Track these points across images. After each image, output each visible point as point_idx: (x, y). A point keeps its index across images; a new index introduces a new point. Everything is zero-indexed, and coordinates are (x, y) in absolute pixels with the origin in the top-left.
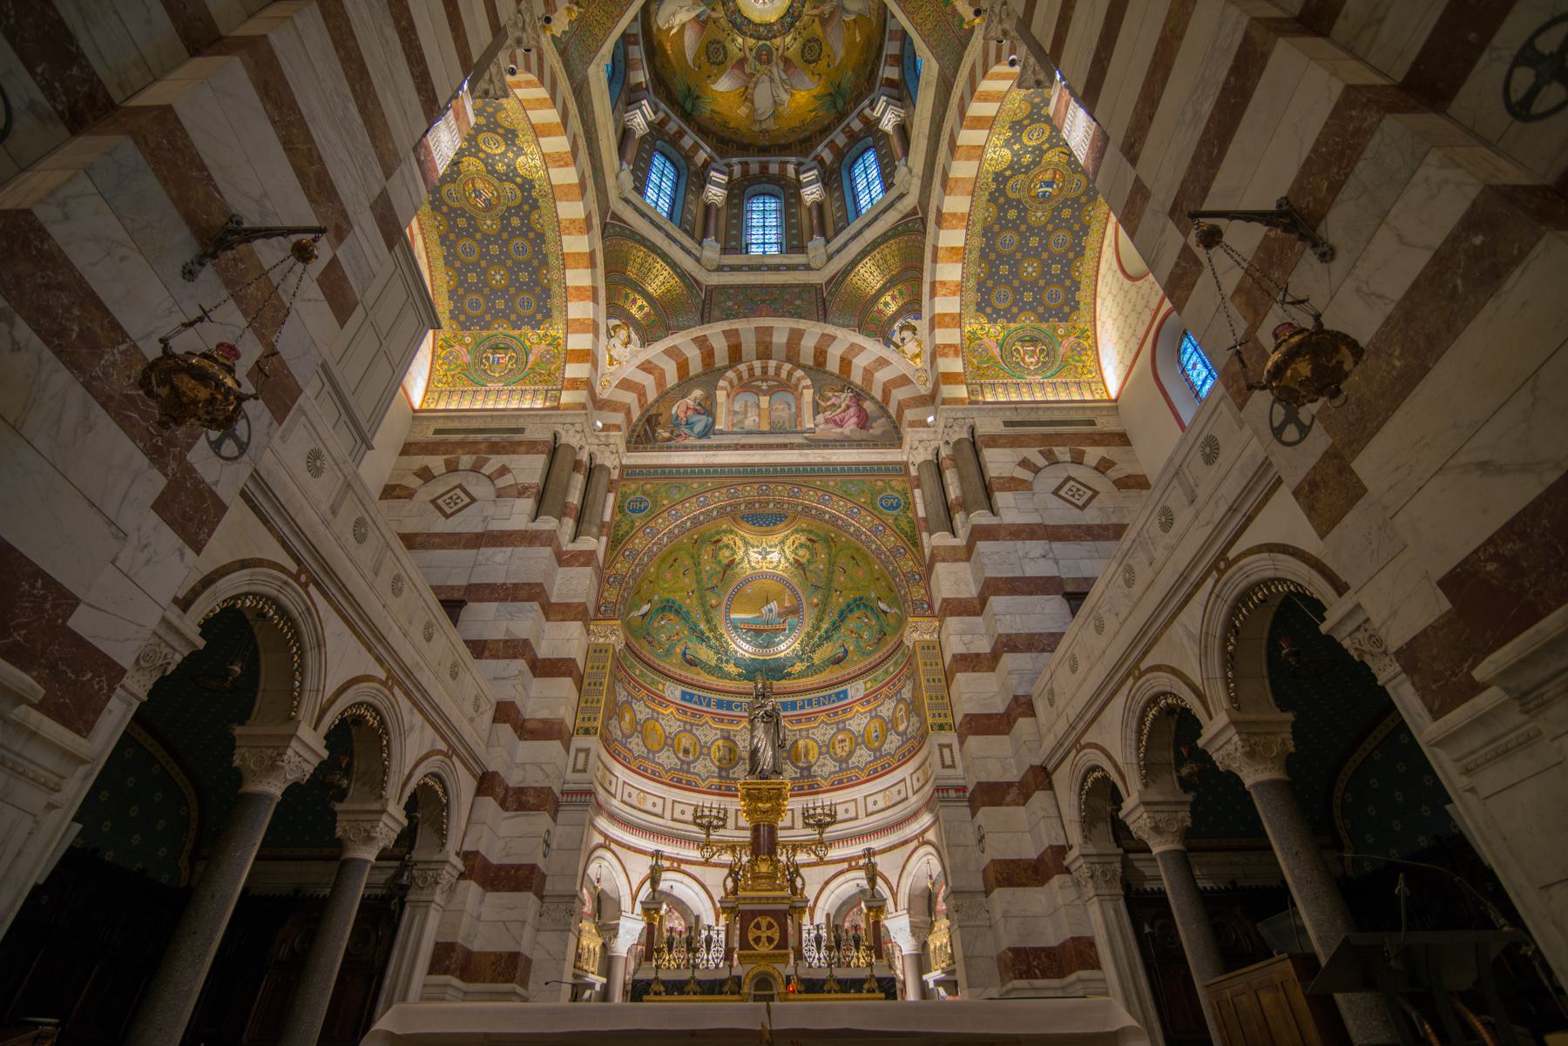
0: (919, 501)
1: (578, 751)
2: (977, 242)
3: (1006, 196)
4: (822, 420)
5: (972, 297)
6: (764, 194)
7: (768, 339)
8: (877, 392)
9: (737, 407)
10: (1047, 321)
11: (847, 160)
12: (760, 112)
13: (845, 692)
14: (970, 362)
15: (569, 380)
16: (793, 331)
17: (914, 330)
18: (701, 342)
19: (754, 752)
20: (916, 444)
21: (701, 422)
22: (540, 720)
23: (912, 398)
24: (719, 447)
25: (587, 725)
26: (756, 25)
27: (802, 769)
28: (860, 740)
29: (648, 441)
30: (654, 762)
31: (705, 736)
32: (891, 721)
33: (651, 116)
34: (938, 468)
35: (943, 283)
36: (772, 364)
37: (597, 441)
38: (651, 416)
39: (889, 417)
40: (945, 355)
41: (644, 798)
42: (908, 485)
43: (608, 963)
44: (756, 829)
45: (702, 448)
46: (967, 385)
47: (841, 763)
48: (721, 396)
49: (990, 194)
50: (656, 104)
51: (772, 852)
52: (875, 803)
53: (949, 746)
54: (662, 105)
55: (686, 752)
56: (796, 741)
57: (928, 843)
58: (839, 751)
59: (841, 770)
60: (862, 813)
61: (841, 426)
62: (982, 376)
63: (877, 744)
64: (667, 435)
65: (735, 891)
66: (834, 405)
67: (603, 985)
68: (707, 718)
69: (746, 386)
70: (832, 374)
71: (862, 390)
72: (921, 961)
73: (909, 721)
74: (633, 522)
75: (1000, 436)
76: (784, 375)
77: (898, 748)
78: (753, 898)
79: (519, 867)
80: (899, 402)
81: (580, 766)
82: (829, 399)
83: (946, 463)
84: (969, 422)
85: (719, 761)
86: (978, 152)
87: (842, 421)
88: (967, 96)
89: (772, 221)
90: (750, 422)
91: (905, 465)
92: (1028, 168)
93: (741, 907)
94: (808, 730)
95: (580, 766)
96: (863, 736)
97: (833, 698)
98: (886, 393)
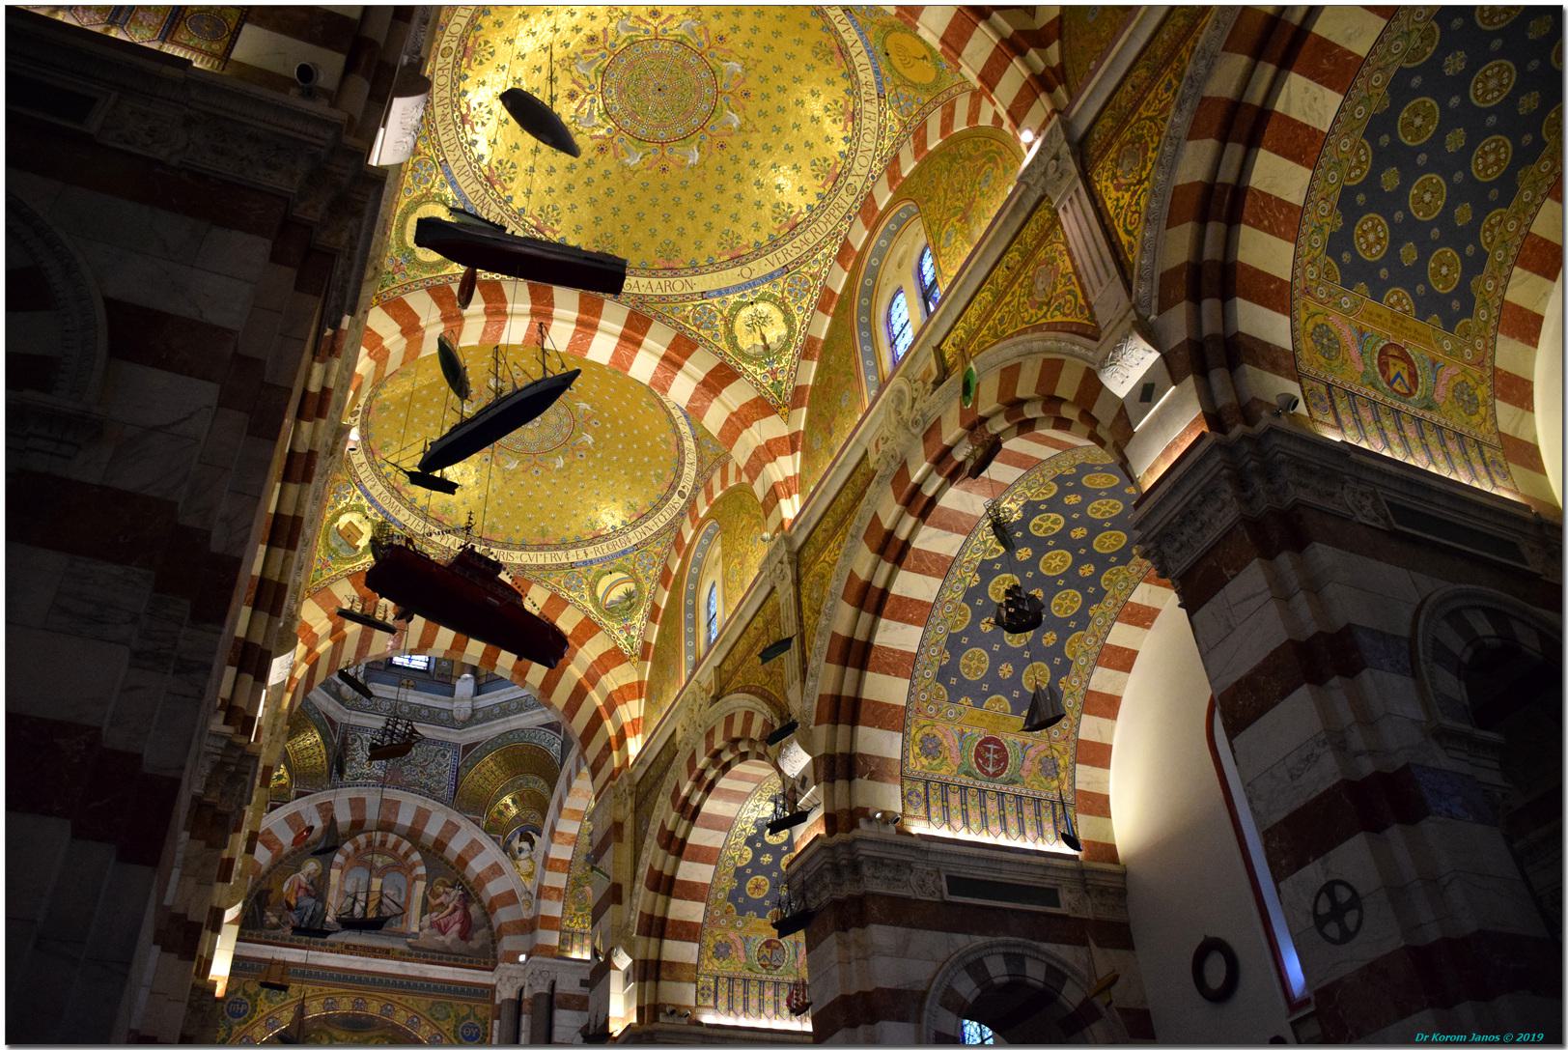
0: (495, 1033)
7: (393, 820)
16: (419, 808)
17: (532, 843)
18: (326, 810)
23: (514, 922)
34: (518, 1004)
35: (562, 834)
36: (392, 838)
38: (262, 892)
39: (491, 928)
40: (549, 898)
42: (489, 1013)
46: (561, 931)
48: (335, 874)
61: (444, 933)
64: (274, 920)
66: (442, 904)
69: (358, 859)
70: (447, 862)
71: (472, 889)
74: (231, 1029)
75: (574, 996)
82: (439, 896)
83: (526, 1007)
84: (552, 976)
87: (446, 926)
91: (492, 988)
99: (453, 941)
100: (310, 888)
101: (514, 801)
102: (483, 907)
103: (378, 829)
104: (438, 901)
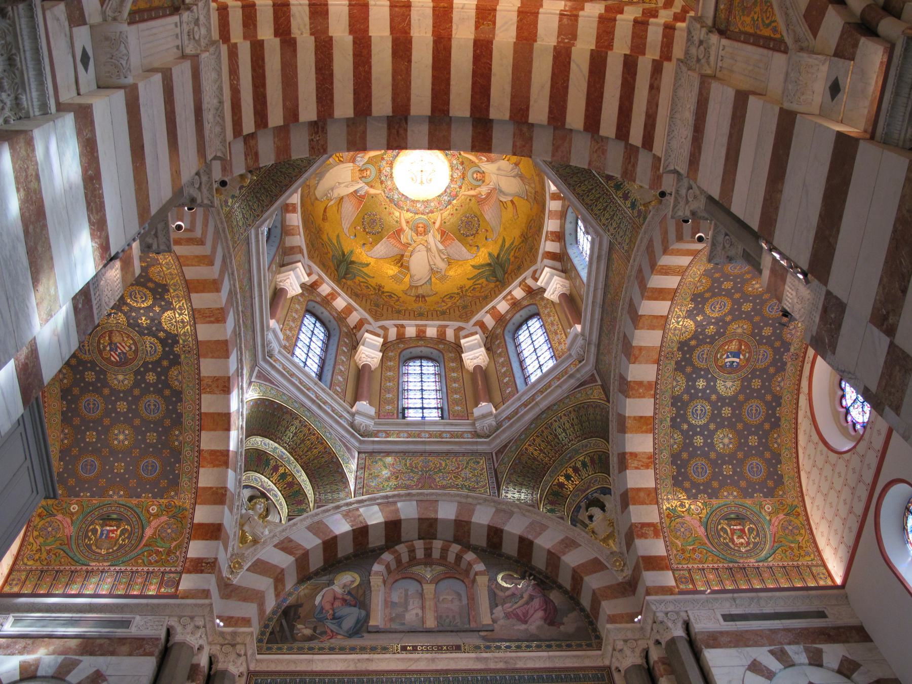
2: (668, 413)
3: (693, 365)
4: (502, 615)
5: (668, 470)
6: (421, 358)
7: (433, 516)
8: (565, 579)
9: (395, 597)
10: (752, 497)
11: (510, 327)
12: (415, 278)
14: (673, 544)
15: (192, 560)
20: (620, 645)
21: (351, 615)
24: (373, 650)
26: (413, 201)
29: (284, 640)
33: (305, 279)
35: (634, 455)
36: (437, 545)
37: (221, 641)
39: (583, 610)
40: (644, 536)
45: (353, 650)
46: (673, 571)
49: (677, 363)
50: (309, 267)
54: (316, 268)
61: (526, 622)
62: (688, 560)
64: (308, 632)
66: (513, 595)
70: (509, 558)
71: (547, 577)
76: (451, 558)
80: (594, 593)
83: (659, 669)
86: (662, 322)
87: (526, 614)
88: (646, 267)
89: (431, 384)
90: (412, 615)
92: (713, 339)
98: (577, 579)
99: (538, 628)
100: (348, 597)
101: (568, 477)
102: (565, 592)
103: (419, 539)
104: (508, 593)
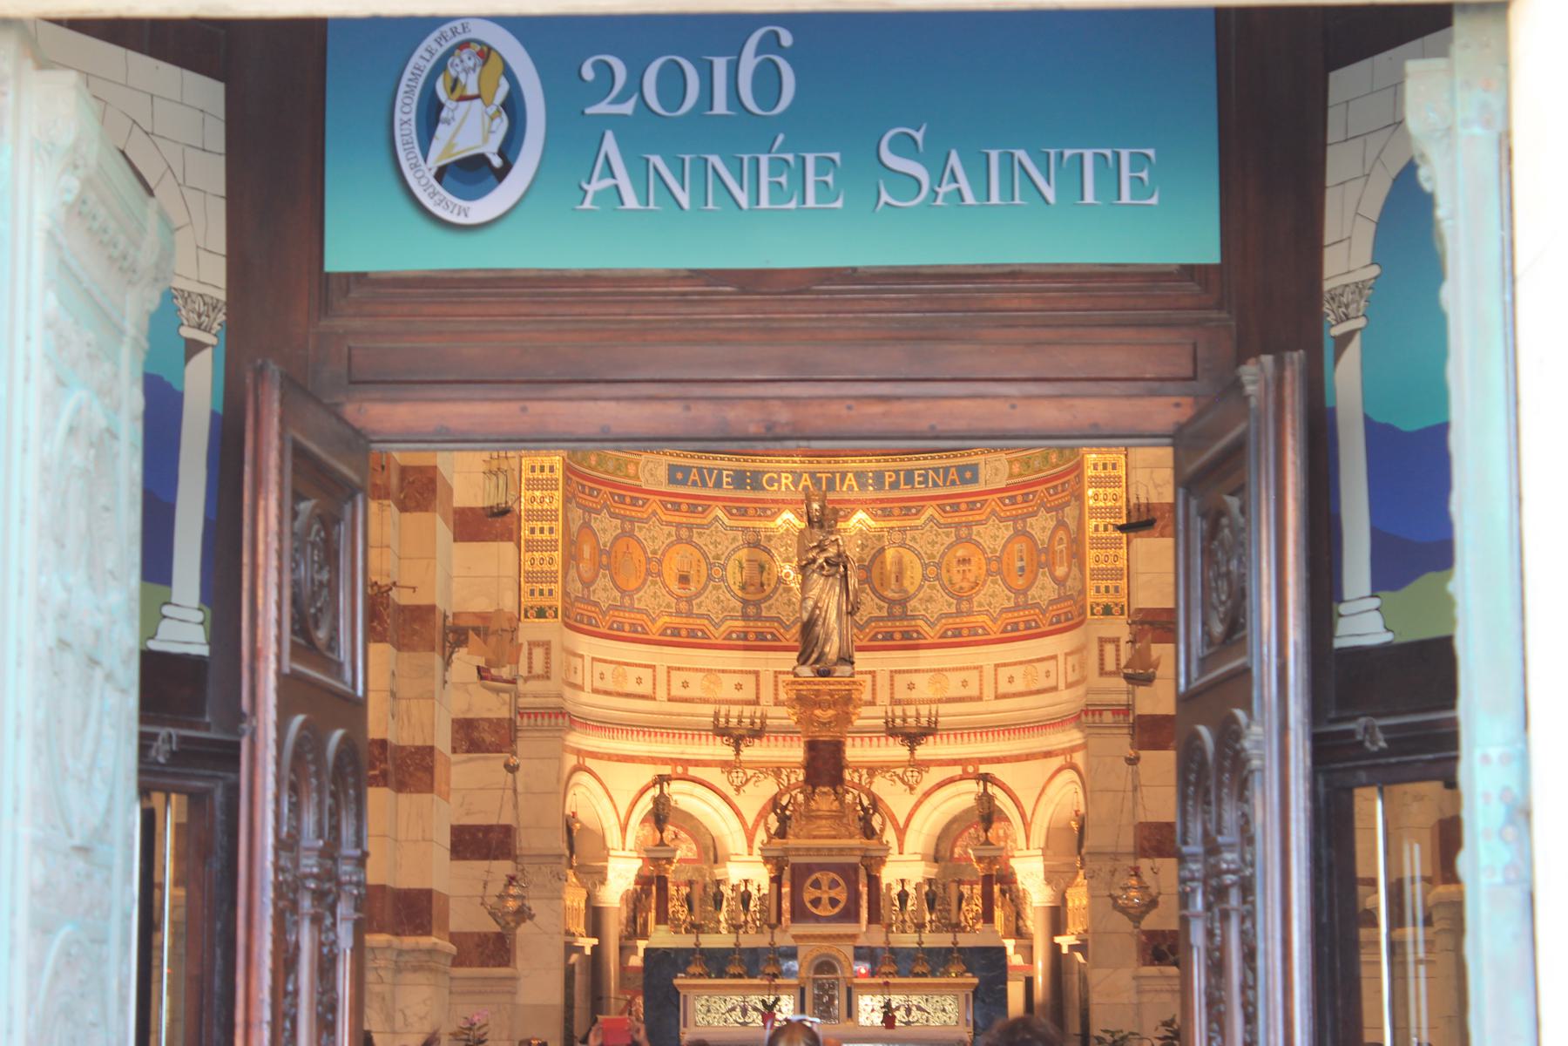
1: (532, 644)
13: (974, 468)
19: (808, 627)
22: (475, 614)
25: (545, 602)
27: (891, 602)
28: (994, 566)
30: (632, 609)
31: (716, 544)
32: (1046, 550)
41: (625, 677)
43: (595, 918)
44: (812, 746)
47: (959, 599)
51: (836, 780)
52: (1011, 680)
53: (1116, 641)
55: (684, 579)
56: (883, 550)
57: (1074, 767)
58: (957, 578)
59: (959, 613)
60: (989, 692)
63: (1021, 582)
65: (782, 833)
67: (594, 948)
68: (720, 514)
72: (1057, 919)
73: (1070, 567)
77: (1052, 602)
78: (808, 849)
79: (488, 829)
81: (538, 668)
85: (743, 588)
93: (793, 860)
94: (903, 530)
95: (538, 668)
96: (999, 559)
97: (953, 475)
